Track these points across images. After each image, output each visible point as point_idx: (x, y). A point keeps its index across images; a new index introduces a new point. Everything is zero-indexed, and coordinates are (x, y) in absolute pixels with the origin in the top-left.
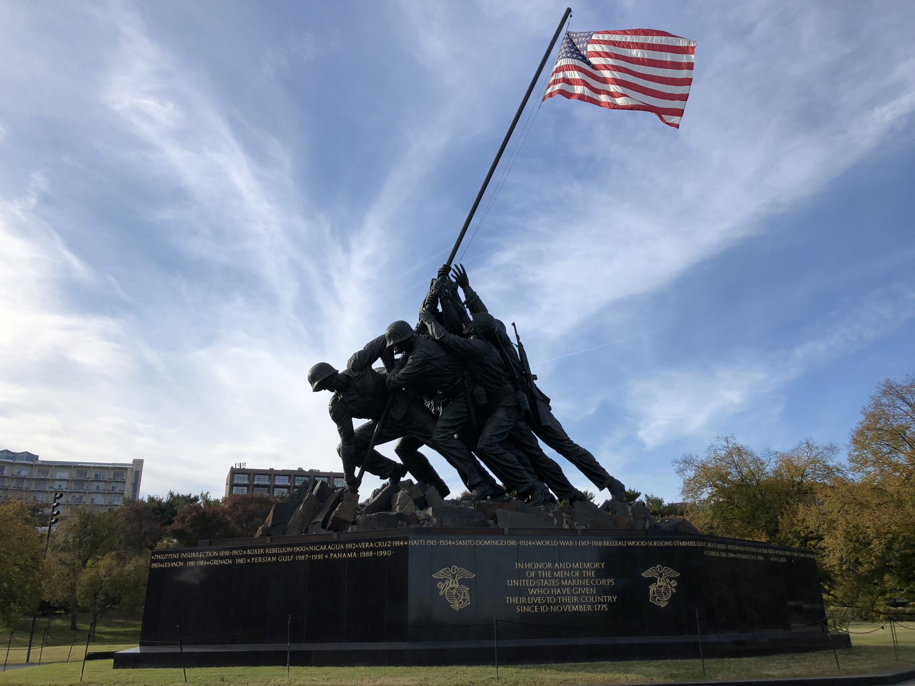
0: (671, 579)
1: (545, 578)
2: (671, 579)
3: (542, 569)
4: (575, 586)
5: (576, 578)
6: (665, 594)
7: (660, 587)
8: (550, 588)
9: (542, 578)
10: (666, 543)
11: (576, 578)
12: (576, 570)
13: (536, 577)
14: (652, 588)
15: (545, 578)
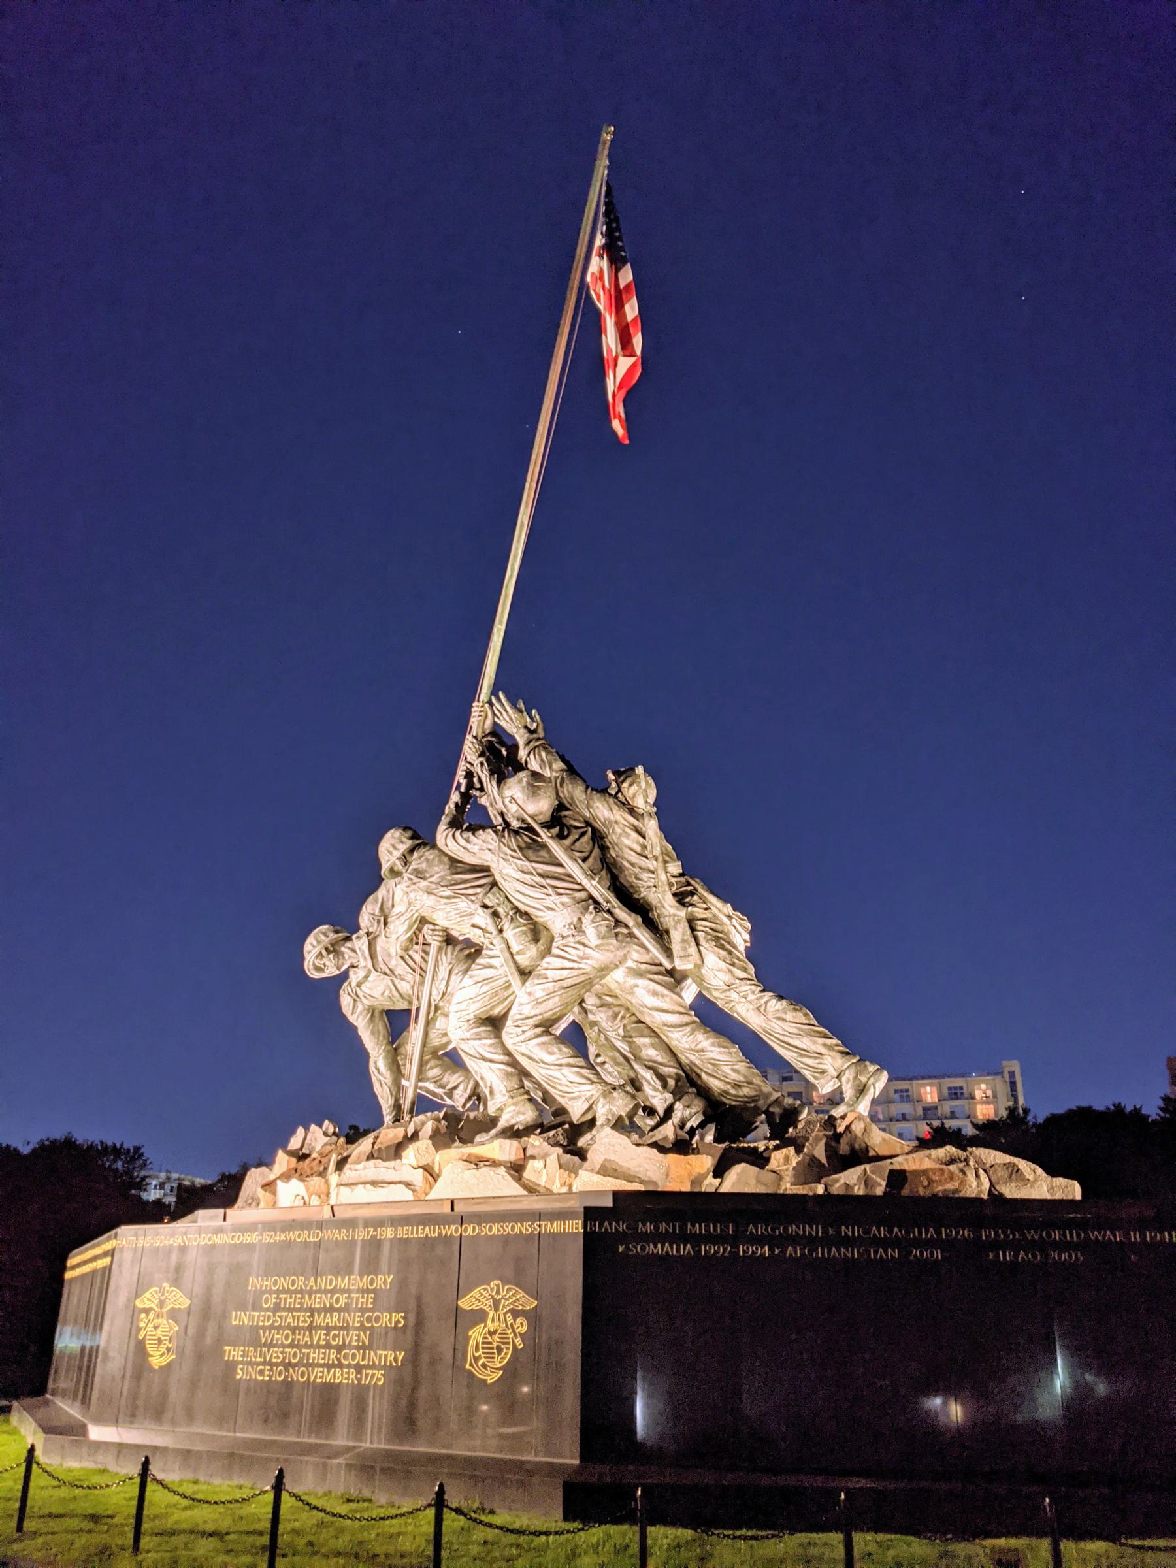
0: (516, 1314)
1: (290, 1310)
2: (516, 1314)
3: (288, 1291)
4: (335, 1328)
5: (339, 1310)
6: (499, 1350)
7: (491, 1333)
8: (293, 1330)
9: (284, 1309)
10: (518, 1228)
11: (339, 1310)
12: (343, 1291)
13: (277, 1308)
14: (476, 1334)
15: (290, 1310)
